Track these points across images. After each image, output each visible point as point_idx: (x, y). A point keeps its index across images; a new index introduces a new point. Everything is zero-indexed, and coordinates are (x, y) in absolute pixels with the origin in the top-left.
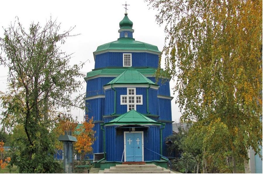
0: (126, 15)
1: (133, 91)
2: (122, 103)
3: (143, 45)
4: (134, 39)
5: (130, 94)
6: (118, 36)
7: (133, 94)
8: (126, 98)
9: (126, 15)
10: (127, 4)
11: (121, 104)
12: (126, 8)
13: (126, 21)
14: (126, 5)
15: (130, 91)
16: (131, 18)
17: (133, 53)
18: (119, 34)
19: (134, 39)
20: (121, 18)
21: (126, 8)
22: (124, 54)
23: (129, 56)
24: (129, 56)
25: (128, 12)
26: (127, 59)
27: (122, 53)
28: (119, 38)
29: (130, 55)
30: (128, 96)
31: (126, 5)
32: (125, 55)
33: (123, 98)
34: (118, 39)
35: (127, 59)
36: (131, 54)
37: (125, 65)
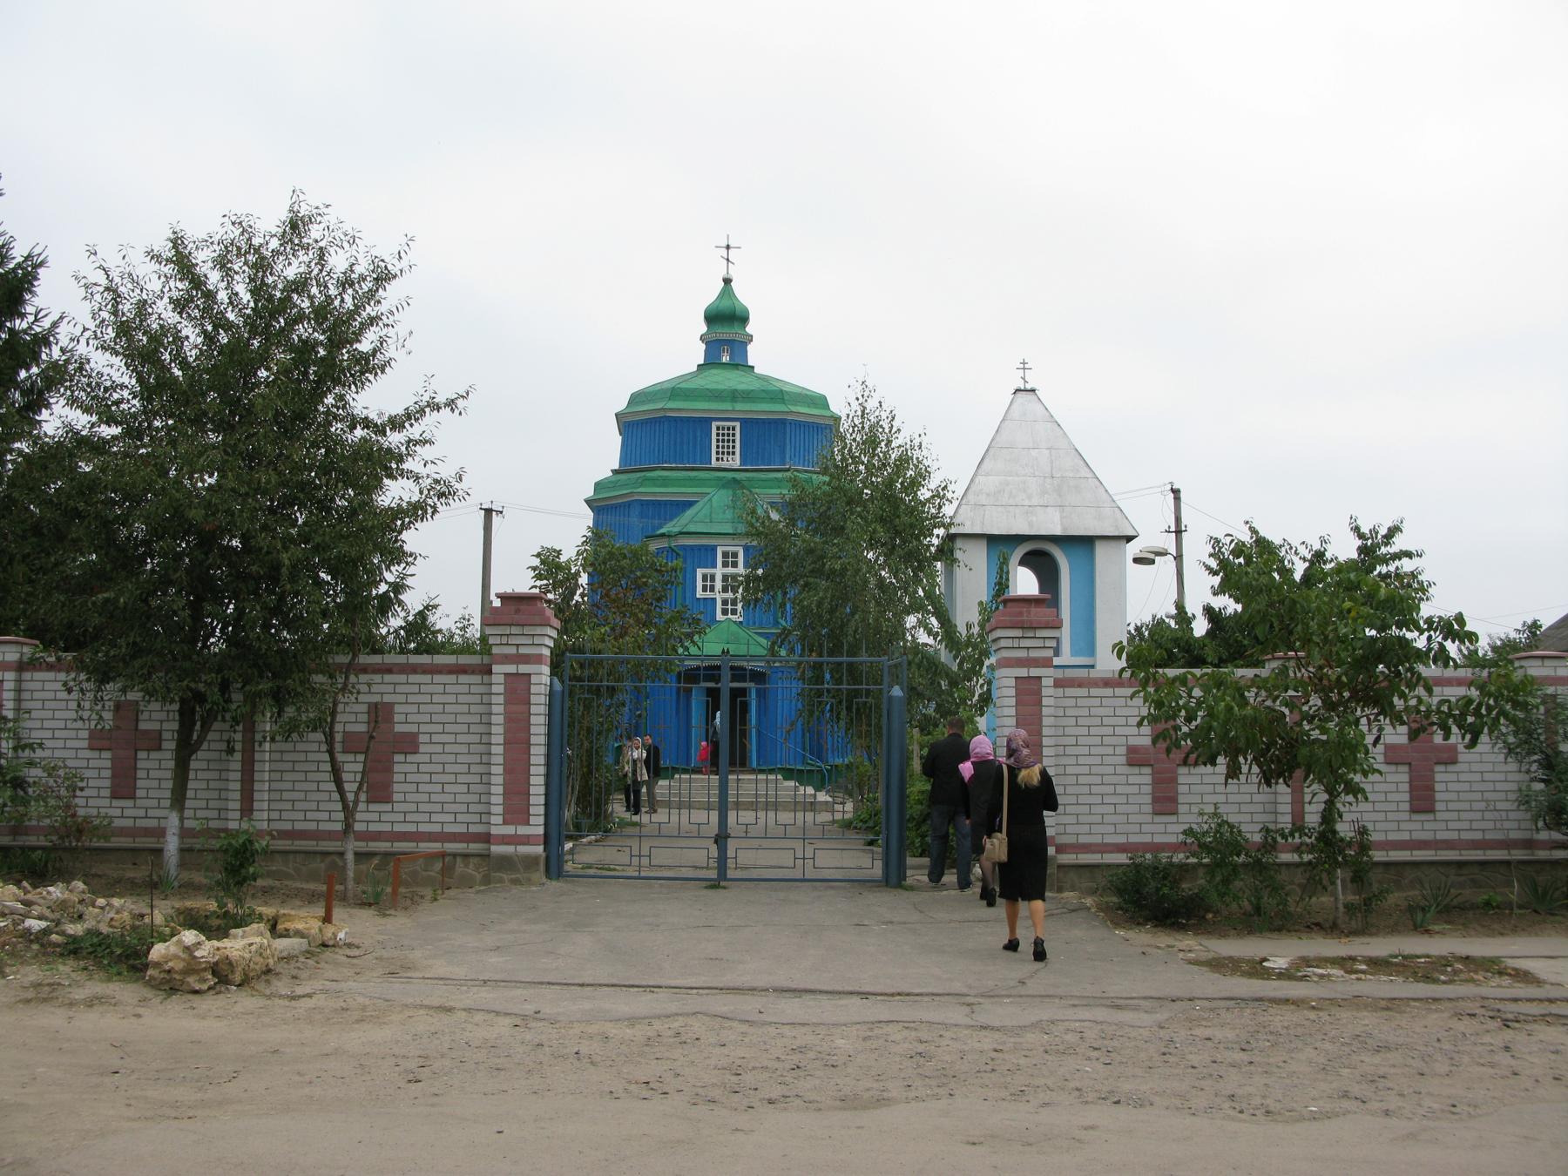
0: (727, 281)
1: (735, 555)
2: (700, 594)
3: (777, 393)
4: (753, 367)
5: (725, 565)
6: (698, 354)
7: (735, 565)
8: (713, 578)
9: (727, 281)
10: (731, 245)
11: (698, 596)
12: (728, 260)
13: (726, 304)
14: (728, 247)
15: (725, 555)
16: (744, 294)
17: (744, 422)
18: (704, 346)
19: (753, 367)
20: (710, 293)
21: (728, 260)
22: (714, 425)
23: (731, 432)
24: (731, 432)
25: (733, 274)
26: (723, 441)
27: (709, 421)
28: (702, 362)
29: (734, 429)
30: (719, 572)
31: (728, 247)
32: (718, 428)
33: (705, 578)
34: (699, 366)
35: (723, 441)
36: (738, 425)
37: (718, 459)
